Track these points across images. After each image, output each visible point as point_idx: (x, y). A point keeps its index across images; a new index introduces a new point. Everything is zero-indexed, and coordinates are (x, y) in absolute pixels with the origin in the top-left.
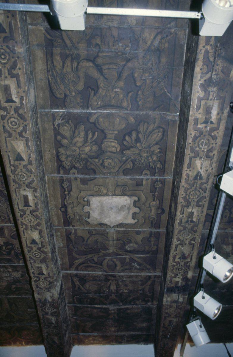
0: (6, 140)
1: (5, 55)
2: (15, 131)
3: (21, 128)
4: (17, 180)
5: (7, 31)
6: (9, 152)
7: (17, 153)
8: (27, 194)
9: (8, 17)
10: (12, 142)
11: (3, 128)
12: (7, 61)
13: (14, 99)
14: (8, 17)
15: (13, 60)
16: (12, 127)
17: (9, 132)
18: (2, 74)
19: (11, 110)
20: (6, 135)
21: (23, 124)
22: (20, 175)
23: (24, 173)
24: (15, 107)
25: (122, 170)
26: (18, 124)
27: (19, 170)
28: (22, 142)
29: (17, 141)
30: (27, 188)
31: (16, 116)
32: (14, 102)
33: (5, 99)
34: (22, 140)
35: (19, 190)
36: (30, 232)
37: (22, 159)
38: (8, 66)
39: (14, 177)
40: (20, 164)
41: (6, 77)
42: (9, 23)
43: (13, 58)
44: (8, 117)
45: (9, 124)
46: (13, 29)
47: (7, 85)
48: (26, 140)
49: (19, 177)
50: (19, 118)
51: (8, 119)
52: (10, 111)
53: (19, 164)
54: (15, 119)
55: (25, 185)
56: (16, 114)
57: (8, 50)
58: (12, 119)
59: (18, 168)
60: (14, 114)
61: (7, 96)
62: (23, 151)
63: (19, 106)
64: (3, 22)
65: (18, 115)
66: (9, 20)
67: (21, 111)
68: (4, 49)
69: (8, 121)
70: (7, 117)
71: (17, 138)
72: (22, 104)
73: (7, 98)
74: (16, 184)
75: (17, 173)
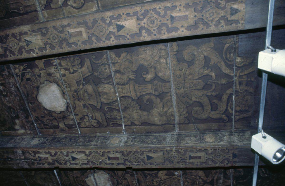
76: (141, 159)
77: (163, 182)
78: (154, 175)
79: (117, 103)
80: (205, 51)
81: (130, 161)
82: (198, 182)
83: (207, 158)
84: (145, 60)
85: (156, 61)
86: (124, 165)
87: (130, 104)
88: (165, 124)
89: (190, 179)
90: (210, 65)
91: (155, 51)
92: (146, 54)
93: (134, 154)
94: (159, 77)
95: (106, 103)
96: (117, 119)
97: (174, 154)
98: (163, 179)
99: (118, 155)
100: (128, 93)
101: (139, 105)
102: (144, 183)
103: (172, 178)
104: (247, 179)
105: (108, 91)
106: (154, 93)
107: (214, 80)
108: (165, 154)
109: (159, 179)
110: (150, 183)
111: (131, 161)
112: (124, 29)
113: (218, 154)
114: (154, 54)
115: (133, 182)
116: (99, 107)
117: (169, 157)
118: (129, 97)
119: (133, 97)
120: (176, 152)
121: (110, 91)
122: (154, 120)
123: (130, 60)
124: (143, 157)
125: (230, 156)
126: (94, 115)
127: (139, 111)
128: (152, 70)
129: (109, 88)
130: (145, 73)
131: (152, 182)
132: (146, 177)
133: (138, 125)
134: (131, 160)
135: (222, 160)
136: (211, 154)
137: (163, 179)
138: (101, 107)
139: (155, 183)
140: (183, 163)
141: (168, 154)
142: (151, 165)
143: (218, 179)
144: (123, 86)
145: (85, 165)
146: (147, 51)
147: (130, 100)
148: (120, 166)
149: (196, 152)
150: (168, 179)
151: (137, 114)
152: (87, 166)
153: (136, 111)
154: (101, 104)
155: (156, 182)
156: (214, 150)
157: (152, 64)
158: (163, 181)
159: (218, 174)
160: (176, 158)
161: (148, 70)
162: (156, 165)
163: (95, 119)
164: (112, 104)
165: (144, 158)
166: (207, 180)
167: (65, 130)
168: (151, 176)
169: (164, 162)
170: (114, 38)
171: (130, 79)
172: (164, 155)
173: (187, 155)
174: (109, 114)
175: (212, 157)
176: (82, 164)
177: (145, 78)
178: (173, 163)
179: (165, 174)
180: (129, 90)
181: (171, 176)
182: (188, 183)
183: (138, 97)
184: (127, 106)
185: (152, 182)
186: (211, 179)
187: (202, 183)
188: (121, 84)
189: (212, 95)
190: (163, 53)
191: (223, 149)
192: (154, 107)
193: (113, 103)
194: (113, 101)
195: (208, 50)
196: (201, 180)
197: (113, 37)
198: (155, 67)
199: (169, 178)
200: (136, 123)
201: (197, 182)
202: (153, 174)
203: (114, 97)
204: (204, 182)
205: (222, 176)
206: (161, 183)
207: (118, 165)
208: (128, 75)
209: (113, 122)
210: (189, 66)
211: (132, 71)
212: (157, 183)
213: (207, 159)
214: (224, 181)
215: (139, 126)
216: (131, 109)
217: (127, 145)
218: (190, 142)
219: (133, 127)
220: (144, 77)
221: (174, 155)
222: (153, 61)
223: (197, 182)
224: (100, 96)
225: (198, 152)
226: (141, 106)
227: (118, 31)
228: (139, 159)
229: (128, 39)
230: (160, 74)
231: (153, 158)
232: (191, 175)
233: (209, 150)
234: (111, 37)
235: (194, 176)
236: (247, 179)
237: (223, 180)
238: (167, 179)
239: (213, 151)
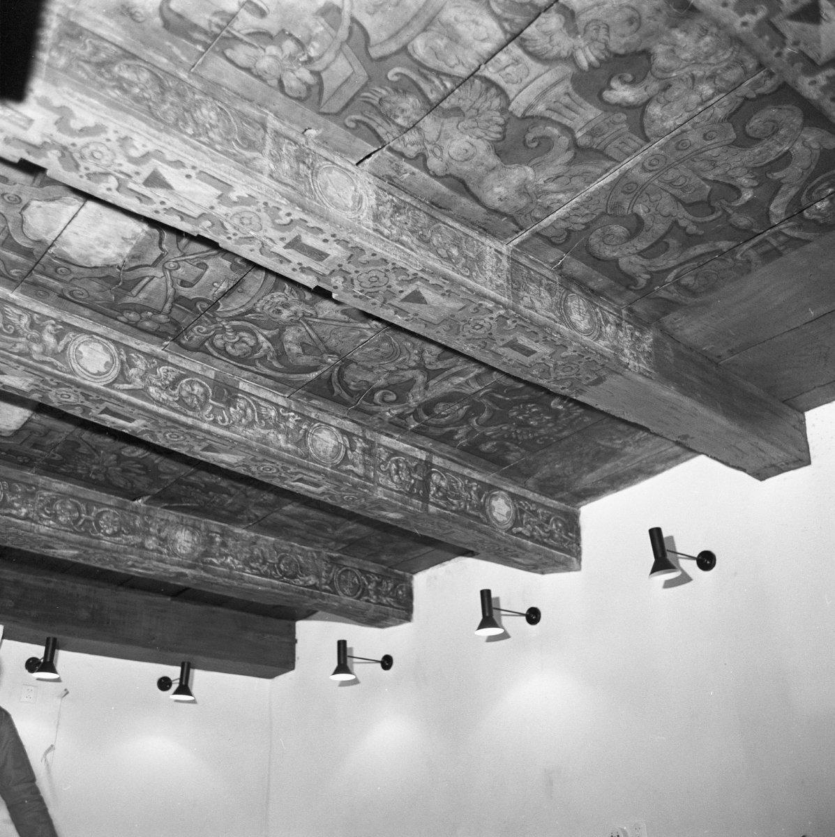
25: (80, 442)
31: (277, 475)
36: (31, 380)
79: (449, 85)
80: (803, 143)
84: (673, 51)
85: (693, 77)
87: (480, 112)
88: (504, 214)
90: (769, 175)
91: (723, 55)
92: (697, 42)
93: (387, 270)
94: (643, 112)
95: (415, 61)
96: (390, 119)
97: (487, 320)
99: (335, 252)
100: (513, 83)
101: (504, 134)
103: (352, 325)
105: (471, 38)
106: (579, 135)
107: (731, 207)
112: (809, 27)
114: (712, 58)
116: (375, 52)
118: (501, 92)
119: (513, 104)
121: (477, 43)
122: (492, 189)
123: (640, 18)
126: (328, 57)
127: (482, 146)
128: (655, 86)
129: (485, 36)
130: (629, 77)
133: (431, 173)
137: (320, 316)
138: (382, 59)
144: (526, 58)
145: (178, 218)
146: (708, 39)
147: (496, 102)
148: (303, 275)
150: (335, 323)
151: (467, 146)
152: (184, 223)
153: (473, 140)
154: (397, 53)
157: (674, 74)
161: (644, 78)
163: (317, 74)
164: (429, 77)
166: (430, 364)
167: (140, 19)
170: (759, 23)
171: (571, 59)
174: (384, 92)
176: (170, 211)
177: (611, 89)
180: (528, 79)
181: (352, 320)
183: (527, 114)
184: (464, 110)
185: (280, 308)
188: (531, 49)
189: (685, 229)
190: (733, 75)
192: (533, 162)
193: (438, 77)
194: (446, 69)
195: (810, 148)
197: (761, 14)
198: (670, 86)
200: (434, 163)
203: (463, 65)
208: (583, 45)
209: (366, 120)
210: (734, 143)
211: (606, 44)
215: (431, 176)
216: (467, 123)
217: (381, 233)
218: (538, 304)
219: (407, 166)
220: (614, 84)
222: (687, 69)
224: (425, 30)
226: (504, 138)
227: (795, 17)
228: (385, 288)
229: (779, 54)
230: (655, 110)
234: (754, 12)
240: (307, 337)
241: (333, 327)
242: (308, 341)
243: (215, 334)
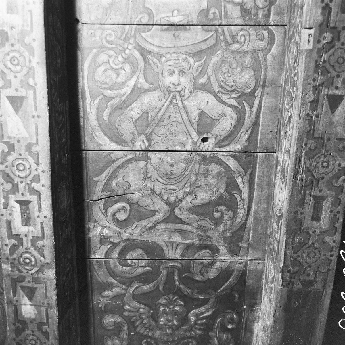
0: (37, 139)
1: (25, 263)
2: (20, 155)
3: (10, 158)
4: (26, 54)
5: (20, 288)
6: (33, 117)
7: (20, 113)
8: (9, 15)
9: (17, 301)
10: (26, 135)
11: (38, 160)
12: (23, 256)
13: (17, 206)
14: (17, 301)
15: (14, 256)
16: (24, 163)
17: (30, 153)
18: (31, 240)
19: (23, 189)
20: (35, 149)
21: (7, 167)
22: (18, 65)
23: (10, 68)
24: (17, 193)
26: (14, 166)
27: (20, 76)
28: (10, 135)
29: (19, 136)
30: (7, 33)
32: (17, 201)
33: (30, 206)
34: (9, 137)
35: (25, 28)
37: (12, 99)
38: (21, 249)
39: (30, 61)
40: (17, 90)
41: (26, 236)
42: (17, 295)
43: (14, 259)
44: (30, 178)
45: (28, 167)
46: (12, 290)
47: (26, 225)
48: (3, 138)
49: (21, 59)
50: (12, 176)
51: (29, 175)
52: (25, 188)
53: (19, 89)
54: (18, 175)
55: (12, 41)
56: (16, 183)
57: (20, 268)
58: (22, 174)
59: (21, 81)
60: (19, 183)
61: (28, 212)
62: (9, 116)
63: (10, 196)
64: (23, 296)
65: (13, 180)
66: (15, 298)
67: (9, 187)
68: (26, 269)
69: (31, 172)
70: (30, 179)
71: (18, 141)
72: (6, 198)
73: (28, 208)
74: (30, 43)
75: (25, 71)
76: (333, 78)
77: (174, 101)
78: (202, 81)
81: (333, 47)
82: (174, 190)
83: (311, 233)
86: (321, 25)
89: (185, 170)
97: (337, 163)
98: (186, 103)
102: (173, 46)
104: (182, 286)
108: (340, 144)
109: (187, 92)
110: (171, 63)
111: (332, 51)
113: (320, 254)
115: (176, 12)
117: (327, 151)
120: (339, 168)
124: (339, 86)
125: (308, 275)
131: (176, 72)
132: (197, 54)
134: (335, 50)
135: (301, 261)
136: (323, 241)
137: (186, 103)
139: (175, 79)
140: (306, 181)
141: (339, 150)
142: (311, 102)
143: (182, 233)
149: (331, 212)
150: (185, 117)
155: (178, 84)
156: (333, 247)
158: (180, 103)
159: (200, 233)
160: (323, 166)
162: (308, 114)
165: (337, 88)
166: (180, 209)
168: (197, 70)
169: (315, 138)
172: (338, 139)
173: (326, 192)
175: (313, 243)
178: (309, 158)
179: (206, 112)
181: (195, 125)
182: (172, 166)
186: (182, 217)
187: (171, 198)
191: (330, 264)
196: (180, 195)
199: (190, 121)
201: (172, 187)
202: (206, 76)
204: (175, 202)
205: (195, 241)
206: (174, 97)
207: (324, 5)
212: (172, 86)
213: (308, 233)
214: (177, 246)
221: (331, 163)
223: (172, 187)
225: (332, 216)
231: (333, 112)
232: (196, 174)
233: (335, 237)
235: (193, 179)
236: (182, 286)
237: (181, 243)
238: (187, 114)
239: (330, 245)
240: (156, 111)
241: (180, 120)
242: (152, 114)
243: (111, 49)
